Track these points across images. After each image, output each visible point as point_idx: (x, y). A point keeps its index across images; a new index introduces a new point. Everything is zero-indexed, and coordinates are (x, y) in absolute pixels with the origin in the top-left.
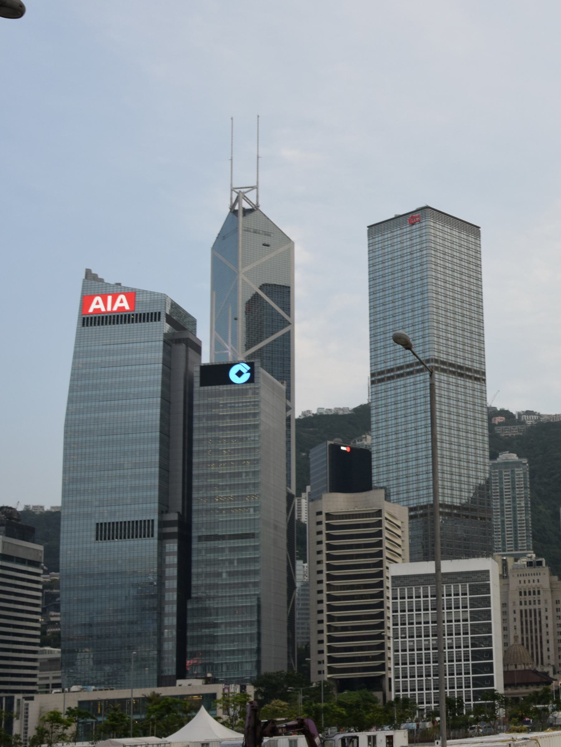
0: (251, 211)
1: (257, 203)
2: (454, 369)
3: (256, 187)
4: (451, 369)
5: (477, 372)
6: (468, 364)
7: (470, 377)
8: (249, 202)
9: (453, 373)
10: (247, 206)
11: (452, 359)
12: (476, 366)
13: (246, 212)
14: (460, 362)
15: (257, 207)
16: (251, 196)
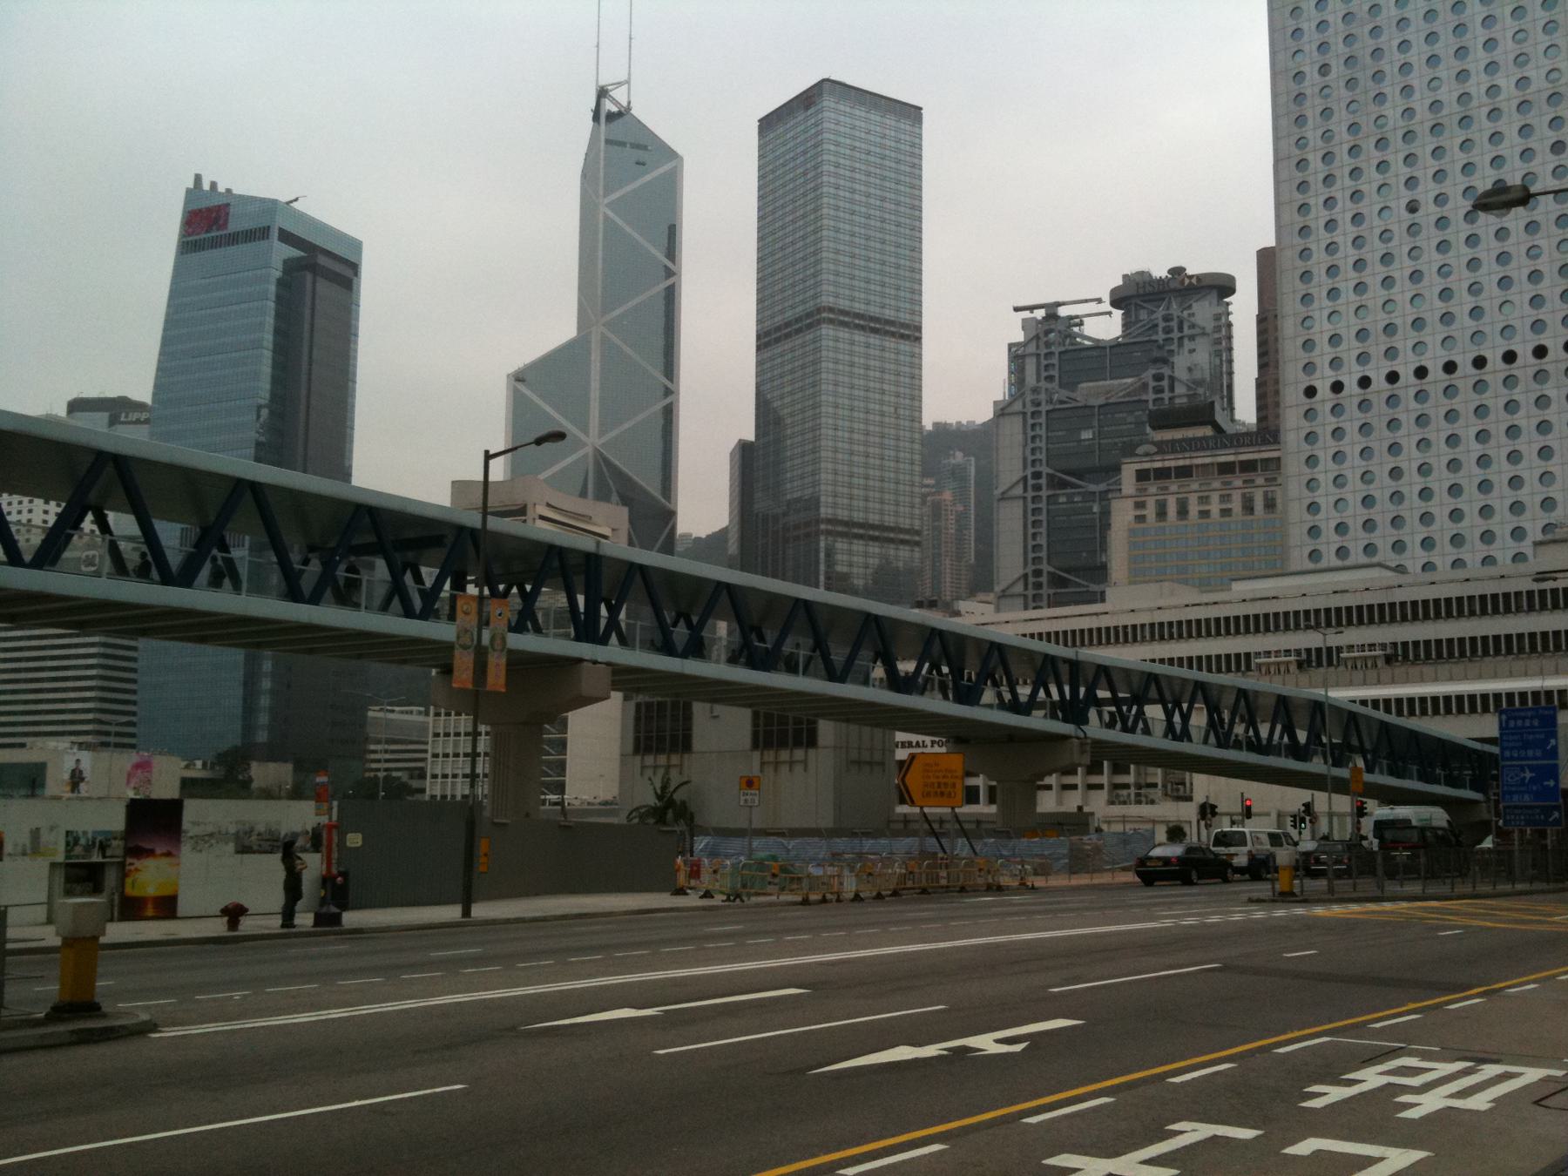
0: (620, 114)
1: (629, 103)
2: (862, 322)
3: (628, 82)
4: (857, 321)
5: (907, 326)
6: (889, 314)
7: (893, 334)
8: (616, 103)
9: (862, 328)
10: (614, 109)
11: (859, 307)
12: (904, 317)
13: (611, 117)
14: (874, 310)
15: (629, 108)
16: (620, 95)
